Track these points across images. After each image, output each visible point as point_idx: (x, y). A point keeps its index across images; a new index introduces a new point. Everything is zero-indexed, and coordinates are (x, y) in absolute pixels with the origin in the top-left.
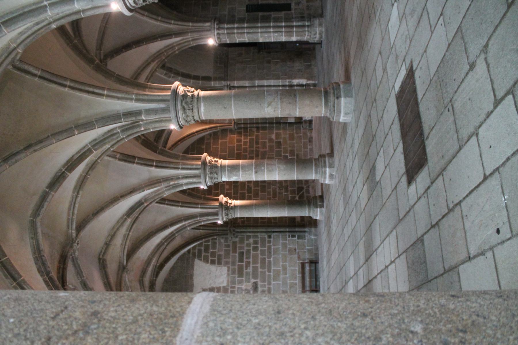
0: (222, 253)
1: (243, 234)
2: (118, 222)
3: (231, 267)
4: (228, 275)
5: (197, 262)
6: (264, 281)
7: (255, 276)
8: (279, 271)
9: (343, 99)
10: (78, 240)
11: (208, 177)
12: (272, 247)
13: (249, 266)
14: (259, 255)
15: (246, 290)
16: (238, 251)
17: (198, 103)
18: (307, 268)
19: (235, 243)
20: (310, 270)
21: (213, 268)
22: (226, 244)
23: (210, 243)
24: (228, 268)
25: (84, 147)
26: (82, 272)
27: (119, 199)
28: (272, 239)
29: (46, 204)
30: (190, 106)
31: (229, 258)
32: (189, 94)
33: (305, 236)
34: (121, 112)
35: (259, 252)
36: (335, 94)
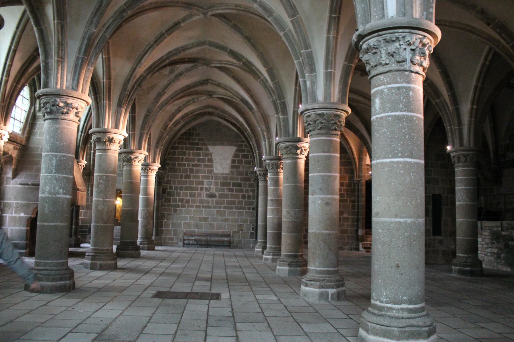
0: (241, 169)
1: (256, 186)
2: (236, 92)
3: (229, 176)
4: (223, 174)
5: (234, 148)
6: (216, 203)
7: (221, 196)
8: (224, 215)
9: (287, 268)
10: (210, 68)
11: (270, 162)
12: (245, 211)
13: (229, 192)
14: (238, 200)
15: (210, 188)
16: (242, 182)
17: (291, 158)
18: (226, 239)
19: (249, 179)
20: (224, 241)
21: (229, 162)
22: (249, 172)
23: (250, 159)
24: (229, 174)
25: (261, 74)
26: (188, 72)
27: (249, 94)
28: (251, 211)
29: (218, 50)
30: (289, 152)
31: (237, 175)
32: (299, 151)
33: (253, 238)
34: (286, 100)
35: (241, 200)
36: (293, 263)
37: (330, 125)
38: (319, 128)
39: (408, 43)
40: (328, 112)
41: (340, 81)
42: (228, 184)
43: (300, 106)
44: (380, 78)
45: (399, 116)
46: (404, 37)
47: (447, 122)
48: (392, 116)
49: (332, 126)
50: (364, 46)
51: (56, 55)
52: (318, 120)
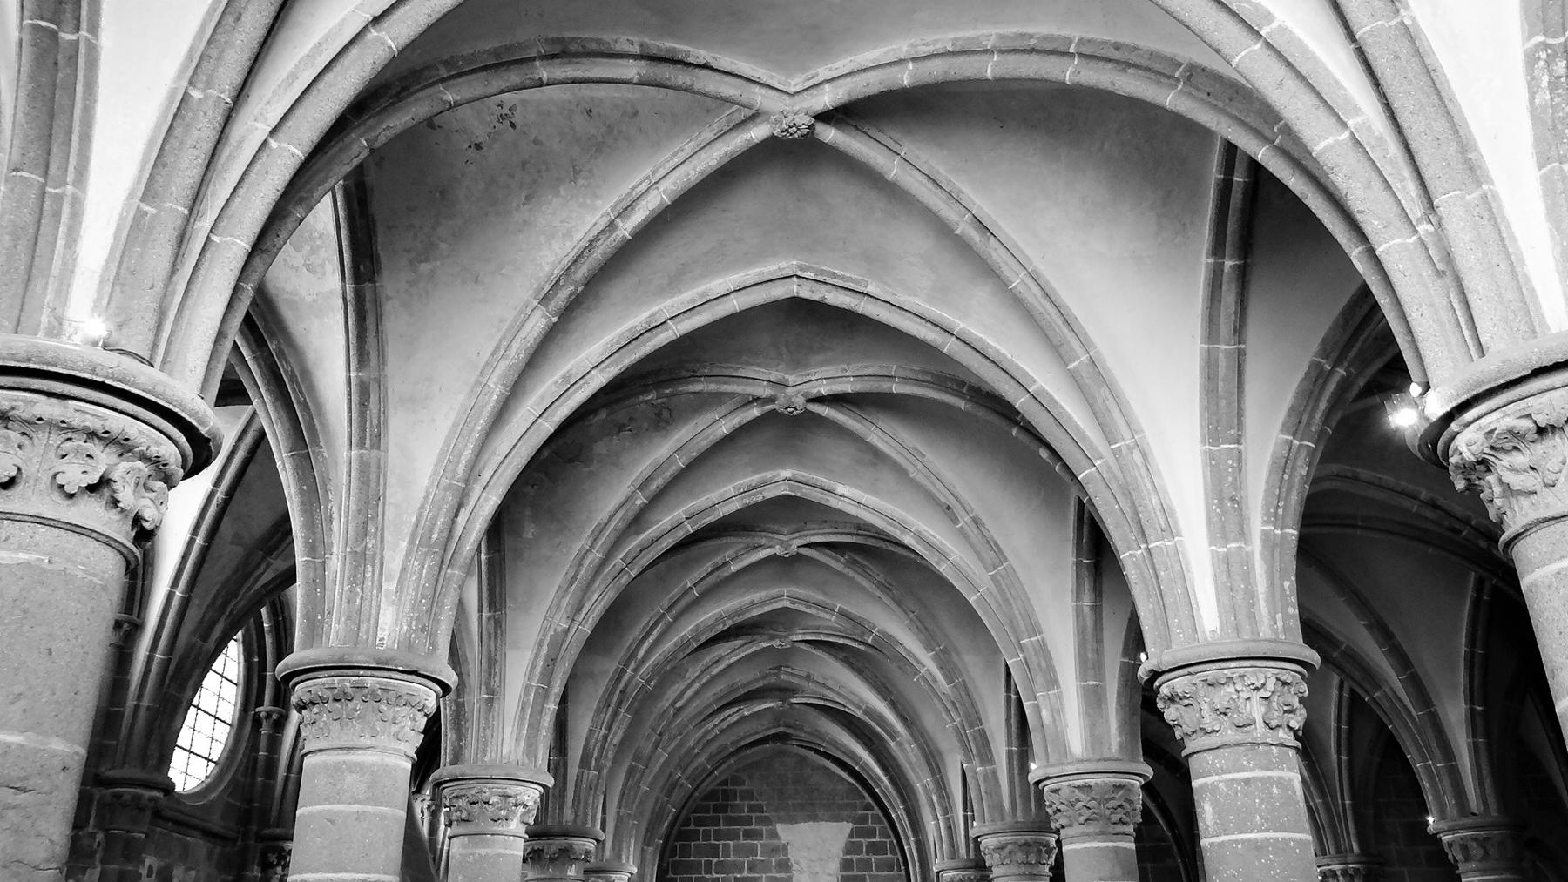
5: (847, 827)
11: (954, 877)
23: (889, 855)
25: (919, 662)
34: (986, 726)
37: (1108, 812)
38: (1082, 819)
39: (1252, 687)
40: (1099, 781)
41: (1118, 702)
43: (1033, 766)
44: (1206, 758)
45: (1256, 841)
46: (1242, 676)
47: (1412, 749)
48: (1243, 841)
49: (1112, 813)
50: (1165, 690)
51: (484, 687)
52: (1078, 800)
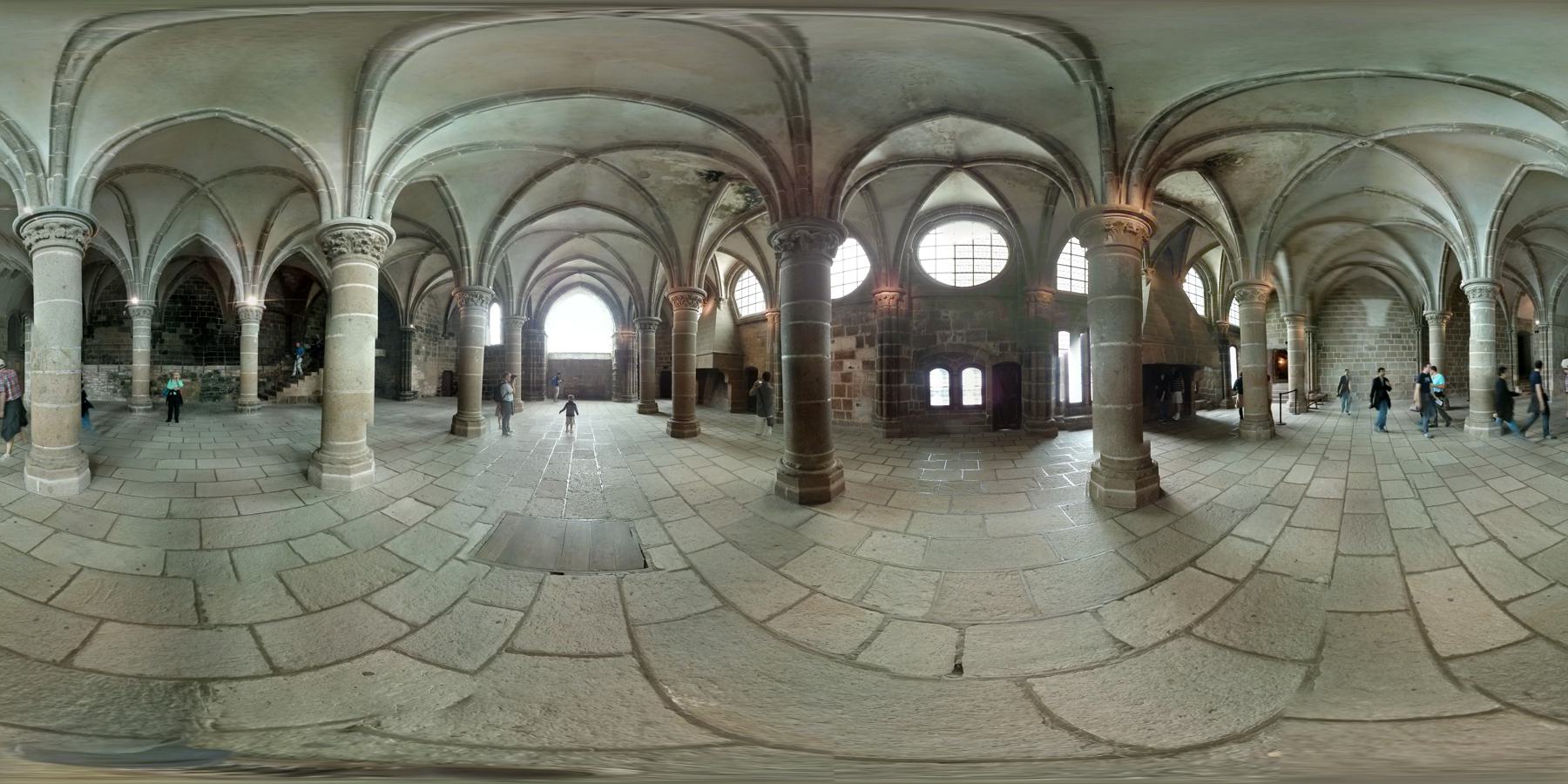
6: (1377, 356)
7: (1380, 348)
42: (1387, 336)
